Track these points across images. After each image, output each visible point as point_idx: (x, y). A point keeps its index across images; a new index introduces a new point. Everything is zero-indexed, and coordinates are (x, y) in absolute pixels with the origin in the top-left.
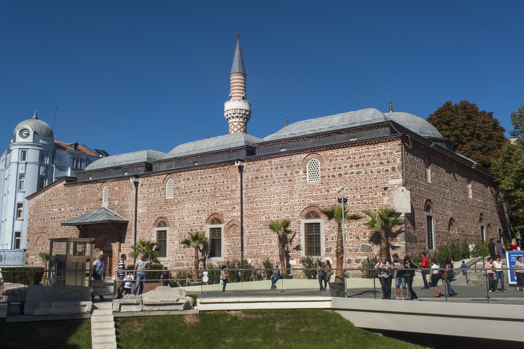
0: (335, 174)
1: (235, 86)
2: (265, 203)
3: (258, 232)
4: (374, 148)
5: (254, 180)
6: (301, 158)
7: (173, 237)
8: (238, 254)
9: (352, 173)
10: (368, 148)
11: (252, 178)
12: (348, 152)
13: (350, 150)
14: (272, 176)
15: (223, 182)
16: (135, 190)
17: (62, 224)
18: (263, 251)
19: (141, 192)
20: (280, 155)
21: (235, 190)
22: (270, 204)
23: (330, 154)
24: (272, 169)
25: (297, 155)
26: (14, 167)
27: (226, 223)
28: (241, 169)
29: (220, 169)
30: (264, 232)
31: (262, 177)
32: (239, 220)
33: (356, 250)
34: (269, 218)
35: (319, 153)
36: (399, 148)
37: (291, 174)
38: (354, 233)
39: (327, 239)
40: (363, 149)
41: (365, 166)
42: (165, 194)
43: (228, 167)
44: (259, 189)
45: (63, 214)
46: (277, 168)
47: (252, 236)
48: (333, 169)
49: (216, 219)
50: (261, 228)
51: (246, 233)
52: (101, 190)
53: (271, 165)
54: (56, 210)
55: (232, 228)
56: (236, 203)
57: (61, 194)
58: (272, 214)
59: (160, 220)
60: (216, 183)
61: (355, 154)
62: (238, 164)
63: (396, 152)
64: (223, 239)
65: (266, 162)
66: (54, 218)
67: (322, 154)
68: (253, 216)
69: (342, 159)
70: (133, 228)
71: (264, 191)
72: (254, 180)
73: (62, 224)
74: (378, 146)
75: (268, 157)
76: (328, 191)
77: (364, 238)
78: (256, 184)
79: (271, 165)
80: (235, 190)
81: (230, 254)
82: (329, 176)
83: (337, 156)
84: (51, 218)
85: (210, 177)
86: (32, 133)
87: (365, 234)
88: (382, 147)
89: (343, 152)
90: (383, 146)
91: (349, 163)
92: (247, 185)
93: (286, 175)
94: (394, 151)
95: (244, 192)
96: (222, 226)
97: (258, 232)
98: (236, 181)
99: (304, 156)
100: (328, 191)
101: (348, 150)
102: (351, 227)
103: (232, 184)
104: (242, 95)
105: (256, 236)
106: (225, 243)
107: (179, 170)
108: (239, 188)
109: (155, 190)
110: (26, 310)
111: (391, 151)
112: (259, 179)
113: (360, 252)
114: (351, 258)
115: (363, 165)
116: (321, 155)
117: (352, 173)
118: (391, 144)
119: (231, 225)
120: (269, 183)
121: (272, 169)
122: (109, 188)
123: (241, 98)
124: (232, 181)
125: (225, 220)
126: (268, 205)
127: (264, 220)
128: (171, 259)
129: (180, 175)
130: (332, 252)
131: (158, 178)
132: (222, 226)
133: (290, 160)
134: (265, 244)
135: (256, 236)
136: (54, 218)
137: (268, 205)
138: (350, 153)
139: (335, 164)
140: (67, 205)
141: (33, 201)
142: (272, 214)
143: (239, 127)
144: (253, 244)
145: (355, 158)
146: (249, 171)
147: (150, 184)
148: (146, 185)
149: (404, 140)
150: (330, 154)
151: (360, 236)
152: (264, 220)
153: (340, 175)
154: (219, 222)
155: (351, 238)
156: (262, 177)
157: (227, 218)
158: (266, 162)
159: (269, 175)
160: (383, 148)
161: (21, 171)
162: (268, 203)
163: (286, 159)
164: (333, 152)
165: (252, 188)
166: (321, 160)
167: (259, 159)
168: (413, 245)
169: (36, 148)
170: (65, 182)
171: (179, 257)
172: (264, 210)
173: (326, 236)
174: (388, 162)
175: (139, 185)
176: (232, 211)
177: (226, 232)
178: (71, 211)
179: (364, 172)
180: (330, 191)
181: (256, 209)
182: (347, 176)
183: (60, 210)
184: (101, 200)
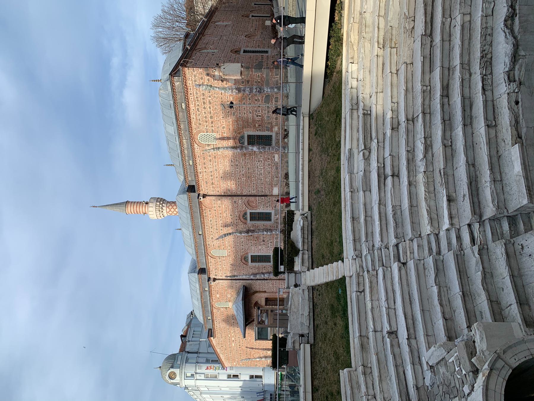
1: (136, 210)
4: (190, 89)
5: (214, 186)
9: (210, 107)
10: (191, 94)
13: (192, 108)
14: (211, 172)
17: (244, 337)
18: (267, 180)
20: (195, 165)
24: (205, 172)
25: (195, 151)
26: (199, 383)
28: (204, 196)
31: (212, 179)
32: (244, 198)
34: (243, 175)
36: (191, 70)
37: (210, 156)
38: (255, 109)
39: (260, 130)
40: (191, 98)
41: (204, 97)
43: (203, 207)
46: (205, 168)
49: (243, 216)
50: (251, 181)
51: (254, 192)
52: (218, 309)
53: (203, 172)
55: (251, 204)
58: (240, 172)
59: (243, 261)
61: (195, 104)
62: (202, 198)
67: (194, 131)
68: (241, 187)
69: (199, 115)
70: (248, 281)
72: (214, 186)
73: (244, 337)
75: (196, 175)
76: (224, 127)
79: (203, 172)
81: (270, 205)
82: (212, 126)
85: (211, 221)
86: (172, 370)
87: (256, 100)
88: (189, 83)
91: (202, 110)
92: (218, 191)
93: (210, 161)
96: (248, 212)
100: (224, 127)
104: (145, 204)
107: (205, 246)
110: (306, 332)
115: (203, 99)
117: (210, 107)
118: (188, 76)
119: (248, 204)
122: (217, 301)
127: (245, 179)
129: (209, 245)
132: (248, 212)
138: (194, 108)
139: (203, 121)
141: (226, 364)
142: (240, 172)
143: (170, 207)
145: (198, 105)
147: (216, 269)
149: (184, 65)
150: (195, 125)
152: (245, 179)
153: (211, 117)
154: (246, 214)
155: (259, 111)
156: (212, 179)
157: (243, 208)
159: (210, 174)
160: (191, 82)
161: (202, 377)
166: (200, 132)
167: (197, 182)
168: (265, 64)
169: (184, 366)
170: (212, 338)
174: (202, 78)
176: (237, 204)
177: (253, 208)
179: (209, 98)
180: (223, 126)
182: (212, 112)
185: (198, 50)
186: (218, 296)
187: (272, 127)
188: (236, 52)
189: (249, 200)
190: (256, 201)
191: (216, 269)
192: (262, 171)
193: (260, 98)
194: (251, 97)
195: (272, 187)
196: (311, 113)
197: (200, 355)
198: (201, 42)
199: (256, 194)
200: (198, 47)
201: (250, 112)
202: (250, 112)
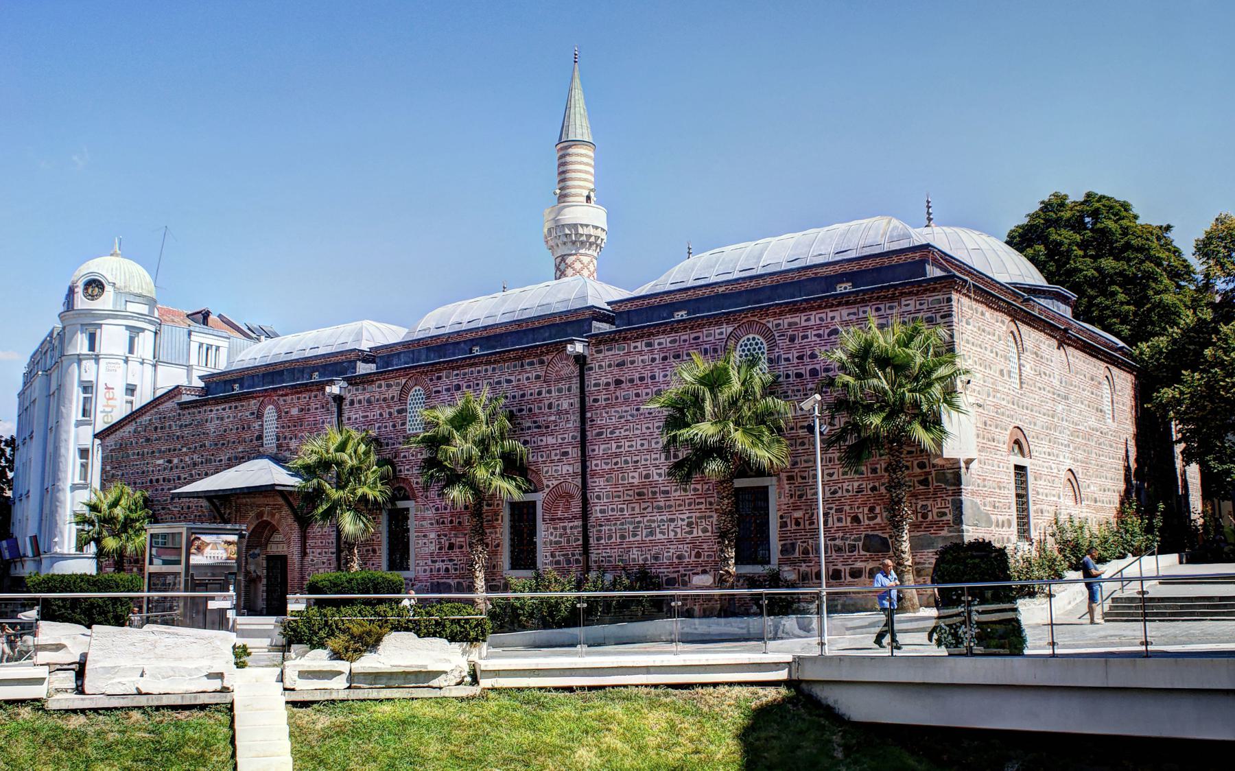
0: (803, 371)
2: (639, 442)
3: (622, 510)
5: (612, 387)
6: (721, 333)
7: (424, 523)
8: (577, 561)
11: (608, 384)
12: (833, 318)
13: (836, 314)
14: (653, 377)
15: (540, 393)
19: (349, 419)
21: (567, 413)
23: (790, 324)
24: (653, 360)
27: (547, 490)
29: (532, 364)
30: (637, 510)
31: (632, 381)
32: (579, 480)
33: (853, 548)
34: (647, 476)
38: (847, 508)
39: (783, 525)
42: (403, 424)
44: (624, 408)
45: (175, 472)
46: (665, 358)
47: (608, 520)
48: (798, 358)
50: (630, 502)
51: (596, 513)
52: (259, 416)
53: (651, 351)
54: (161, 462)
56: (569, 443)
57: (170, 426)
60: (523, 395)
63: (942, 317)
64: (541, 527)
65: (639, 344)
66: (157, 481)
67: (771, 323)
69: (819, 336)
72: (612, 387)
74: (900, 304)
77: (870, 519)
78: (617, 398)
79: (651, 351)
81: (558, 562)
82: (788, 376)
83: (806, 328)
84: (151, 481)
85: (509, 381)
87: (872, 509)
89: (821, 319)
90: (912, 302)
92: (596, 401)
94: (938, 316)
95: (589, 415)
96: (539, 498)
97: (622, 510)
98: (569, 390)
99: (730, 329)
101: (831, 314)
102: (840, 494)
104: (586, 193)
105: (617, 519)
106: (544, 534)
108: (578, 406)
109: (381, 415)
111: (930, 314)
112: (623, 385)
113: (862, 553)
114: (840, 567)
116: (770, 325)
119: (561, 496)
121: (653, 360)
122: (279, 410)
124: (560, 390)
125: (545, 482)
127: (636, 481)
128: (421, 575)
129: (439, 378)
130: (797, 555)
131: (389, 386)
132: (539, 498)
133: (695, 338)
134: (638, 538)
135: (617, 519)
136: (157, 481)
139: (803, 347)
140: (184, 450)
141: (111, 441)
142: (657, 467)
144: (610, 537)
146: (600, 367)
147: (369, 401)
148: (360, 402)
151: (861, 516)
155: (840, 520)
158: (640, 345)
159: (647, 374)
162: (645, 442)
163: (686, 337)
164: (797, 320)
165: (607, 405)
171: (439, 570)
172: (635, 458)
173: (781, 517)
175: (347, 402)
176: (560, 461)
178: (195, 464)
181: (617, 455)
183: (170, 462)
184: (260, 437)
185: (1014, 329)
186: (294, 411)
187: (793, 563)
188: (1017, 442)
189: (572, 497)
190: (570, 520)
191: (369, 401)
192: (659, 536)
193: (878, 520)
194: (881, 495)
196: (804, 686)
197: (148, 369)
198: (1041, 336)
199: (592, 519)
200: (1024, 329)
201: (835, 492)
202: (835, 492)
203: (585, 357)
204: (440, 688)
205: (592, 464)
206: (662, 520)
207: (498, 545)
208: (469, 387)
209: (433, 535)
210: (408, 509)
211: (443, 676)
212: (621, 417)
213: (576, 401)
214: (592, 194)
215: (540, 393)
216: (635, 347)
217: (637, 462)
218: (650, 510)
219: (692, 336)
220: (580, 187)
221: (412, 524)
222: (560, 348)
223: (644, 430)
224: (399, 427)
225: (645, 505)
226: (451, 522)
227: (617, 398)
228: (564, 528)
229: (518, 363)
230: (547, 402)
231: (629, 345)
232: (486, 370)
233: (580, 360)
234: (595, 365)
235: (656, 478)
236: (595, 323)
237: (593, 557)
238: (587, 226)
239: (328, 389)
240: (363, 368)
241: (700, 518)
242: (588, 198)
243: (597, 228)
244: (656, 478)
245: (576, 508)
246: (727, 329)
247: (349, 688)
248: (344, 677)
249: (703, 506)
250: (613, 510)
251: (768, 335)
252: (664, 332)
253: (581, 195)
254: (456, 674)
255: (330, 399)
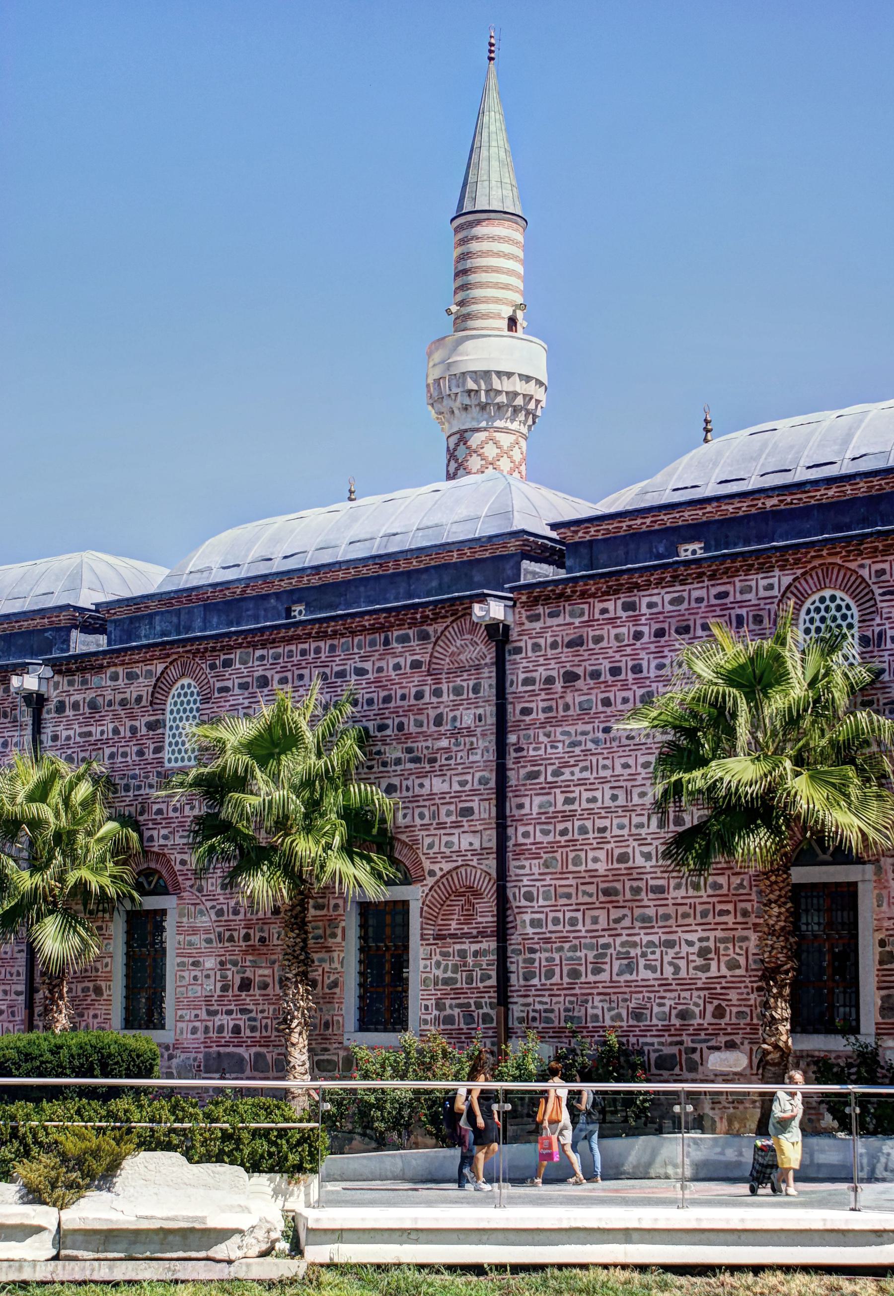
2: (608, 793)
5: (558, 686)
6: (770, 587)
7: (194, 938)
8: (486, 1018)
11: (550, 680)
14: (637, 669)
15: (419, 696)
16: (29, 731)
19: (55, 738)
21: (471, 733)
22: (628, 793)
24: (638, 636)
27: (430, 881)
29: (404, 639)
32: (491, 864)
35: (853, 565)
42: (158, 750)
44: (581, 727)
46: (660, 633)
47: (547, 941)
50: (590, 906)
51: (524, 925)
53: (635, 620)
60: (387, 699)
64: (417, 950)
65: (610, 605)
68: (553, 847)
71: (601, 735)
72: (558, 686)
78: (567, 707)
79: (635, 620)
80: (471, 733)
81: (449, 1020)
85: (360, 672)
92: (526, 711)
95: (512, 738)
97: (573, 922)
98: (476, 689)
99: (787, 580)
103: (456, 706)
104: (507, 311)
105: (565, 939)
106: (423, 965)
108: (491, 720)
109: (116, 731)
112: (580, 684)
116: (865, 573)
120: (625, 701)
121: (638, 636)
123: (504, 324)
124: (458, 691)
125: (427, 865)
126: (621, 801)
127: (601, 867)
129: (227, 664)
131: (131, 676)
133: (719, 596)
134: (604, 976)
135: (565, 939)
137: (621, 801)
144: (550, 974)
146: (536, 647)
147: (93, 705)
148: (76, 706)
159: (626, 663)
163: (702, 593)
165: (548, 722)
171: (221, 1029)
172: (600, 823)
173: (882, 943)
175: (52, 705)
176: (457, 825)
181: (568, 817)
189: (477, 894)
190: (474, 939)
191: (93, 705)
195: (558, 1033)
199: (515, 939)
203: (507, 628)
204: (230, 1262)
205: (517, 835)
206: (651, 944)
207: (335, 984)
208: (283, 681)
209: (210, 963)
210: (164, 912)
211: (236, 1238)
212: (574, 744)
213: (489, 711)
214: (520, 315)
215: (419, 696)
216: (604, 611)
217: (603, 830)
218: (627, 922)
219: (714, 591)
220: (497, 301)
221: (171, 939)
222: (458, 611)
223: (619, 770)
224: (149, 755)
225: (615, 914)
226: (247, 937)
227: (567, 707)
228: (462, 954)
229: (380, 638)
230: (432, 713)
231: (591, 607)
232: (318, 651)
233: (498, 634)
234: (526, 643)
235: (640, 861)
236: (526, 564)
237: (517, 1011)
238: (509, 375)
239: (15, 681)
240: (82, 643)
241: (724, 940)
242: (512, 322)
243: (527, 379)
244: (640, 861)
245: (486, 917)
246: (782, 579)
247: (56, 1258)
248: (47, 1238)
249: (729, 919)
250: (556, 921)
251: (861, 592)
252: (659, 583)
253: (499, 316)
254: (260, 1234)
255: (19, 700)
